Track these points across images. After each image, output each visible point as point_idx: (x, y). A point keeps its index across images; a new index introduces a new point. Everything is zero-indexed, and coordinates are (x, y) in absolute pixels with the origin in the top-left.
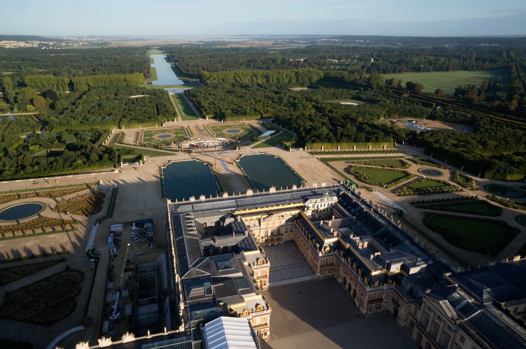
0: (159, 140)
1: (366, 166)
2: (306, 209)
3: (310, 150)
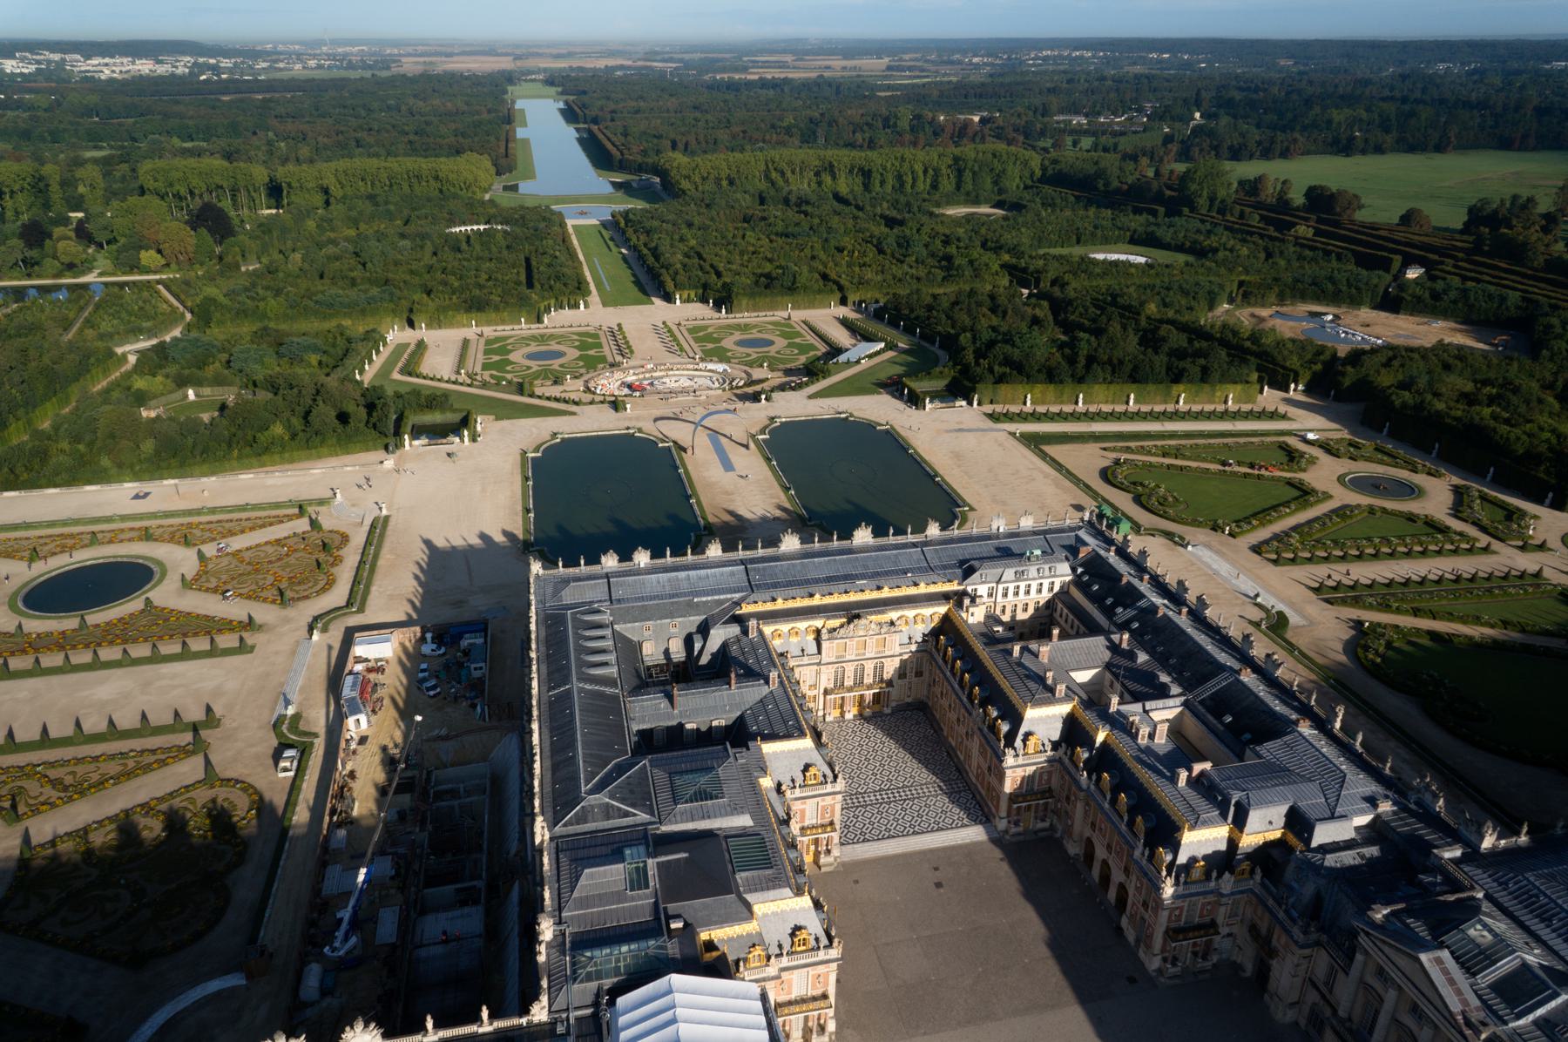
0: (529, 368)
2: (967, 601)
3: (988, 408)
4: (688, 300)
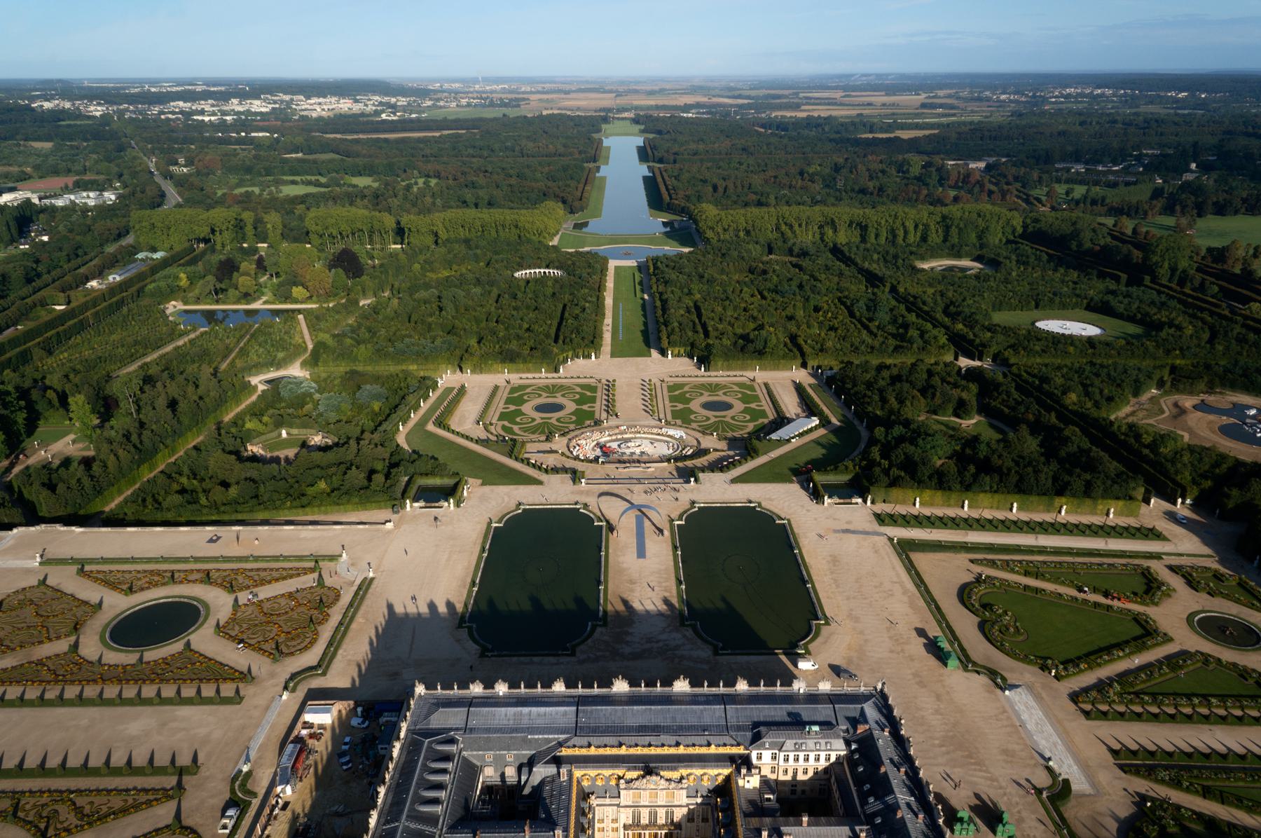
0: (534, 420)
4: (679, 355)
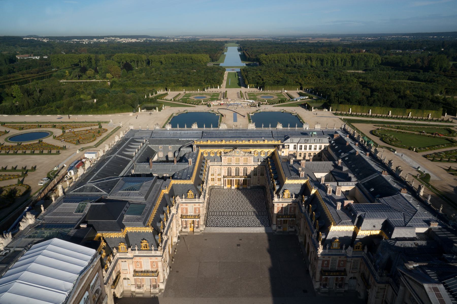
1: (398, 130)
4: (252, 87)
